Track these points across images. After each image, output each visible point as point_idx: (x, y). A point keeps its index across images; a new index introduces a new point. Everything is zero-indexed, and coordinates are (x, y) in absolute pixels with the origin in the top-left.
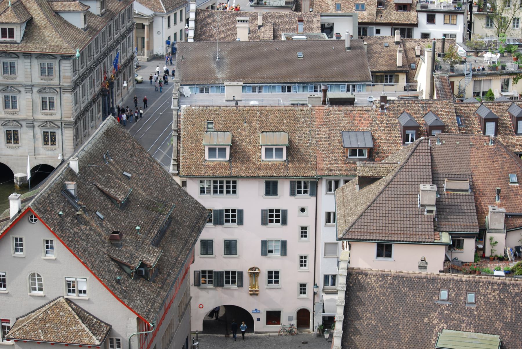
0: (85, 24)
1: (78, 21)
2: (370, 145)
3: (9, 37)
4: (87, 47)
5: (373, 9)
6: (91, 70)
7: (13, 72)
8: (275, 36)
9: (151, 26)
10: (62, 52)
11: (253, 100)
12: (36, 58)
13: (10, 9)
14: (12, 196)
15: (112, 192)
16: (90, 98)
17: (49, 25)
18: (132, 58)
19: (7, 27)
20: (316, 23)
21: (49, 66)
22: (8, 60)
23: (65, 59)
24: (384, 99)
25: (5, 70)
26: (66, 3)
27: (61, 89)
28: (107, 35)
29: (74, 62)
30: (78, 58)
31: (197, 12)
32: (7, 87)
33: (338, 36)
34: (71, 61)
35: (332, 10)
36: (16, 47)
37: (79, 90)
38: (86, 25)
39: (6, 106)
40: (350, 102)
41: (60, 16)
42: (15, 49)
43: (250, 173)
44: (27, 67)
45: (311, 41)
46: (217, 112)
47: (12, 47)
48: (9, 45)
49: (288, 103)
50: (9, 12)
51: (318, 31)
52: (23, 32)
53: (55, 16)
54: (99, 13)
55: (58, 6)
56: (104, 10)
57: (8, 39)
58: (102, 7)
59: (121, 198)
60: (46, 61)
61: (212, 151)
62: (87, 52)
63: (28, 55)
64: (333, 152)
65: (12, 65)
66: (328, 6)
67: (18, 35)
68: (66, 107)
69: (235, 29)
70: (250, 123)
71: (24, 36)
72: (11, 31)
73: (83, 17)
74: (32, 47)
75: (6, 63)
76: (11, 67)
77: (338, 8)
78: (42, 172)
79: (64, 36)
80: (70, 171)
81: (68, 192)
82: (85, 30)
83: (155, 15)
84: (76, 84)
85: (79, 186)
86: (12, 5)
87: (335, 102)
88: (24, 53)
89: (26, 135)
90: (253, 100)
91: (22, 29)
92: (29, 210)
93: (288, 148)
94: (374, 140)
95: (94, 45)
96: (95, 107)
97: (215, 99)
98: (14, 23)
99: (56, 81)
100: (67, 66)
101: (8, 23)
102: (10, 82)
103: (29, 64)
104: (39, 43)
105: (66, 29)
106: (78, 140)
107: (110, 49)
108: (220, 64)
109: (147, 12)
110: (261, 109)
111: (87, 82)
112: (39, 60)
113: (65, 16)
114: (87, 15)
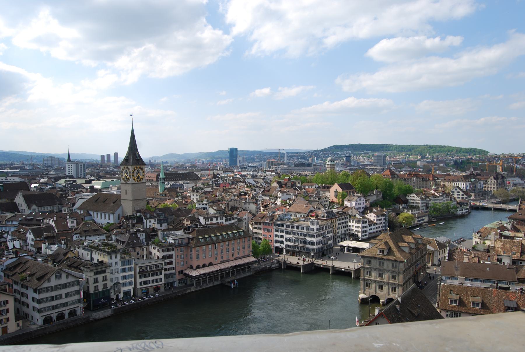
1: (407, 250)
2: (516, 306)
5: (519, 254)
6: (410, 267)
7: (383, 265)
8: (479, 262)
9: (433, 254)
10: (400, 260)
11: (469, 284)
14: (377, 307)
15: (413, 311)
16: (409, 276)
17: (396, 250)
18: (425, 265)
20: (495, 258)
24: (522, 289)
27: (399, 273)
31: (449, 250)
32: (380, 270)
33: (504, 263)
35: (502, 253)
37: (405, 274)
39: (380, 276)
40: (508, 289)
43: (466, 311)
45: (493, 264)
46: (455, 287)
49: (483, 286)
51: (496, 261)
55: (400, 244)
59: (416, 314)
60: (395, 263)
61: (452, 301)
64: (500, 307)
66: (500, 252)
68: (400, 279)
69: (463, 258)
70: (467, 292)
72: (383, 251)
74: (390, 257)
77: (504, 253)
78: (390, 300)
79: (401, 254)
80: (398, 301)
81: (396, 309)
83: (435, 250)
84: (404, 272)
85: (400, 307)
87: (501, 288)
89: (386, 288)
90: (469, 284)
92: (382, 313)
93: (481, 303)
94: (517, 304)
96: (411, 280)
97: (456, 283)
99: (397, 270)
100: (402, 265)
102: (382, 268)
106: (403, 290)
107: (418, 261)
108: (457, 270)
109: (432, 249)
110: (471, 288)
111: (408, 271)
113: (402, 248)
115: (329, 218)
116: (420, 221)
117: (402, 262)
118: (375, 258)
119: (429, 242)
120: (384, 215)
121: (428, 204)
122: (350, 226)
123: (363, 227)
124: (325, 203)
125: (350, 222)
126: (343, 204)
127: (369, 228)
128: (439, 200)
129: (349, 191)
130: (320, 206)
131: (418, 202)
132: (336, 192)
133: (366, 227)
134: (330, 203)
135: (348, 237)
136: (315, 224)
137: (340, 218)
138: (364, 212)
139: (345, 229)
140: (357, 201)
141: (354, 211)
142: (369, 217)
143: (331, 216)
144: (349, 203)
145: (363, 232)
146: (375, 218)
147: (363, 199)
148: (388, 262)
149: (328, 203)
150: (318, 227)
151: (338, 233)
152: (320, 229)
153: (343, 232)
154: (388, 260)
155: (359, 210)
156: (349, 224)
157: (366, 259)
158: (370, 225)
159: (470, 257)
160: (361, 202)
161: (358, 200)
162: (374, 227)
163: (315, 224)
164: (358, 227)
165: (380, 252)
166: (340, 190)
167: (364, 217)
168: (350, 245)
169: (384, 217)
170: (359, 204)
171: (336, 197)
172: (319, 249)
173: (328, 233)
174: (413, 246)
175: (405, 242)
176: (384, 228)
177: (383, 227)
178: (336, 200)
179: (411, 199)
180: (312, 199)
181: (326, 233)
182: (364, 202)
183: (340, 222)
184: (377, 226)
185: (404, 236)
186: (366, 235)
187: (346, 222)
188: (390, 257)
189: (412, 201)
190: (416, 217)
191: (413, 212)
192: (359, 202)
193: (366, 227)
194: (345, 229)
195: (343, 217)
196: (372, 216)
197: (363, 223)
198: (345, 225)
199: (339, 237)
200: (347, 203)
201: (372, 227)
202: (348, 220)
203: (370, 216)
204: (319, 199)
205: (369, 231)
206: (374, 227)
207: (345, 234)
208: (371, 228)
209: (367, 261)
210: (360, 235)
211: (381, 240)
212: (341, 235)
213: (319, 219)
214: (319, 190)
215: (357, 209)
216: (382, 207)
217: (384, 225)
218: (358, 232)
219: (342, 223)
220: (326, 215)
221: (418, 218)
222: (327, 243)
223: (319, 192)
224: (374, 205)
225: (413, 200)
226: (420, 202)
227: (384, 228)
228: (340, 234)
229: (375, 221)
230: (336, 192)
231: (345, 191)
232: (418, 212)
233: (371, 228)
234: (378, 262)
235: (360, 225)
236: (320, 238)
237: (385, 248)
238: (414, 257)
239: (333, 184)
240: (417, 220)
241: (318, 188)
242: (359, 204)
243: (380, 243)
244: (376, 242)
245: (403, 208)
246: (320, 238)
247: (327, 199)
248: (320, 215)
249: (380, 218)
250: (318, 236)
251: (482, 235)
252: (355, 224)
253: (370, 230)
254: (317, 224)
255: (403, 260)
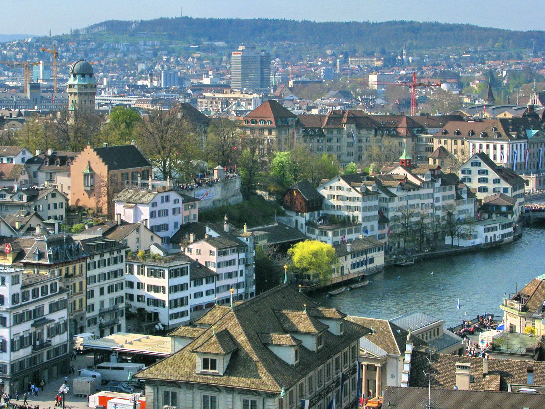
0: (296, 360)
3: (211, 369)
4: (298, 384)
12: (239, 393)
13: (213, 339)
19: (210, 357)
21: (253, 404)
22: (209, 394)
23: (270, 397)
25: (206, 405)
26: (276, 335)
28: (324, 374)
29: (281, 401)
30: (284, 396)
34: (277, 399)
36: (218, 380)
38: (298, 361)
41: (268, 349)
42: (216, 382)
44: (228, 403)
47: (213, 380)
48: (210, 377)
50: (212, 341)
52: (226, 364)
53: (263, 349)
54: (315, 349)
56: (321, 346)
57: (209, 371)
58: (319, 343)
60: (250, 398)
62: (298, 391)
63: (230, 390)
65: (213, 400)
67: (221, 368)
71: (227, 369)
72: (214, 362)
73: (294, 352)
75: (207, 397)
76: (211, 401)
82: (296, 367)
86: (216, 334)
88: (226, 387)
91: (225, 361)
95: (307, 384)
98: (217, 354)
101: (210, 353)
103: (231, 400)
104: (242, 377)
105: (274, 364)
109: (379, 352)
112: (242, 396)
114: (301, 349)
115: (59, 260)
116: (358, 265)
117: (273, 395)
118: (190, 385)
119: (366, 331)
120: (241, 247)
121: (386, 209)
122: (131, 285)
123: (174, 289)
124: (52, 212)
125: (131, 272)
126: (111, 215)
127: (193, 290)
128: (419, 196)
129: (130, 170)
130: (34, 222)
131: (353, 204)
132: (91, 175)
133: (182, 287)
134: (69, 210)
135: (123, 321)
136: (8, 279)
137: (97, 258)
138: (176, 240)
139: (115, 295)
140: (154, 205)
141: (145, 235)
142: (194, 256)
143: (64, 253)
144: (130, 212)
145: (174, 303)
146: (214, 259)
147: (174, 196)
148: (229, 397)
149: (62, 212)
150: (17, 289)
151: (91, 308)
152: (25, 298)
153: (107, 306)
154: (230, 390)
155: (163, 234)
156: (127, 277)
157: (162, 390)
158: (197, 281)
159: (475, 374)
160: (170, 206)
161: (158, 199)
162: (212, 286)
163: (8, 279)
164: (157, 289)
165: (205, 366)
166: (101, 169)
167: (181, 256)
168: (128, 348)
169: (242, 255)
170: (160, 213)
171: (90, 193)
172: (21, 363)
173: (54, 308)
174: (310, 344)
175: (287, 332)
176: (241, 291)
177: (238, 286)
178: (90, 203)
179: (332, 197)
180: (8, 198)
181: (46, 310)
182: (180, 205)
183: (96, 272)
184: (220, 283)
185: (285, 312)
186: (182, 314)
187: (115, 274)
188: (236, 381)
189: (336, 202)
190: (345, 254)
191: (339, 238)
192: (161, 207)
193: (182, 287)
194: (115, 295)
195: (107, 256)
196: (202, 252)
197: (174, 273)
198: (113, 281)
199: (92, 321)
200: (124, 213)
201: (204, 287)
202: (121, 266)
203: (199, 251)
204: (30, 199)
205: (193, 302)
206: (212, 286)
207: (114, 312)
208: (198, 289)
209: (166, 394)
210: (164, 314)
211: (209, 326)
212: (102, 314)
213: (26, 265)
214: (35, 168)
215: (155, 229)
216: (238, 222)
217: (241, 279)
218: (156, 302)
219: (105, 276)
220: (48, 251)
221: (354, 254)
222: (48, 344)
223: (35, 175)
224: (211, 217)
225: (340, 197)
226: (359, 204)
227: (241, 291)
228: (96, 312)
229: (214, 269)
230: (91, 175)
231: (118, 172)
232: (353, 236)
233: (198, 289)
234: (199, 396)
235: (163, 282)
236: (25, 328)
237: (220, 350)
238: (315, 380)
239: (78, 148)
240: (350, 261)
241: (31, 161)
242: (160, 213)
243: (204, 338)
244: (196, 335)
245: (308, 223)
246: (25, 328)
247: (59, 200)
248: (28, 251)
249: (228, 258)
250: (19, 319)
251: (529, 305)
252: (147, 280)
253: (196, 295)
254: (15, 280)
255: (276, 388)
